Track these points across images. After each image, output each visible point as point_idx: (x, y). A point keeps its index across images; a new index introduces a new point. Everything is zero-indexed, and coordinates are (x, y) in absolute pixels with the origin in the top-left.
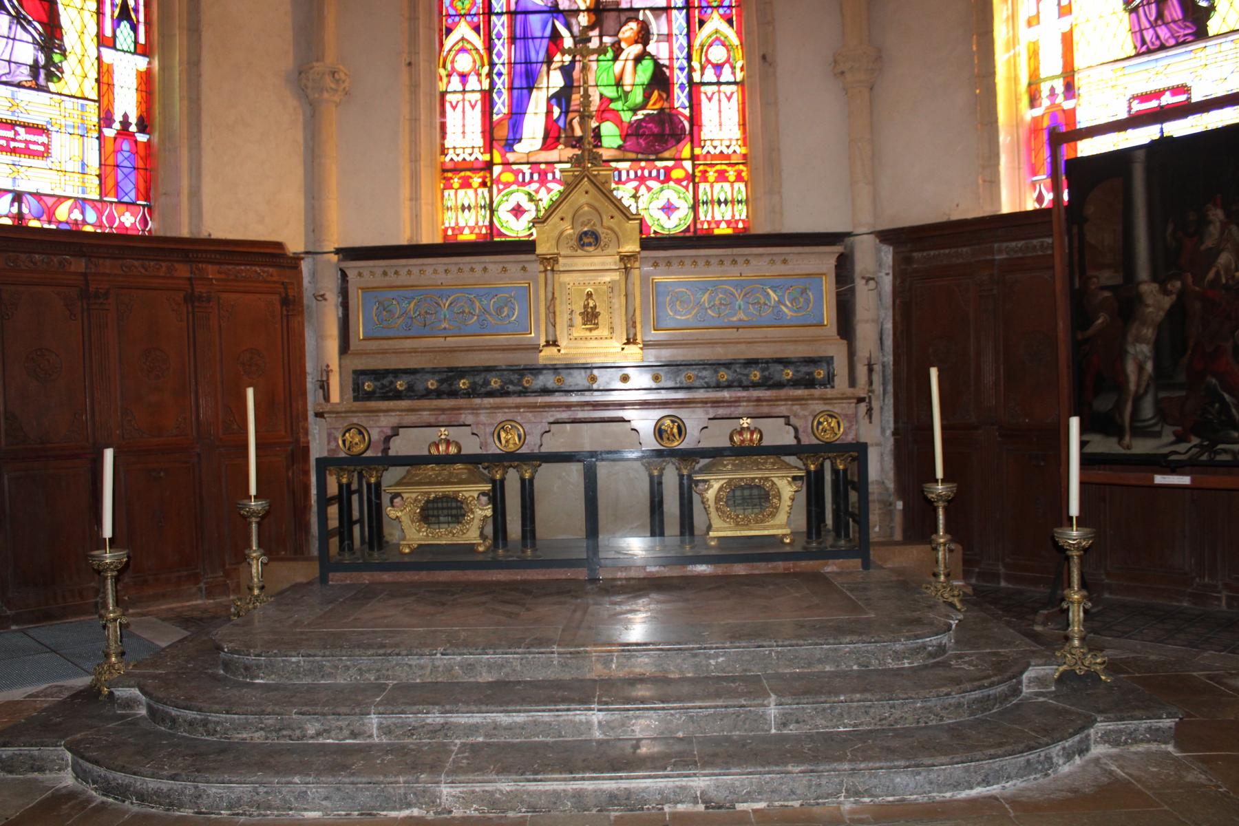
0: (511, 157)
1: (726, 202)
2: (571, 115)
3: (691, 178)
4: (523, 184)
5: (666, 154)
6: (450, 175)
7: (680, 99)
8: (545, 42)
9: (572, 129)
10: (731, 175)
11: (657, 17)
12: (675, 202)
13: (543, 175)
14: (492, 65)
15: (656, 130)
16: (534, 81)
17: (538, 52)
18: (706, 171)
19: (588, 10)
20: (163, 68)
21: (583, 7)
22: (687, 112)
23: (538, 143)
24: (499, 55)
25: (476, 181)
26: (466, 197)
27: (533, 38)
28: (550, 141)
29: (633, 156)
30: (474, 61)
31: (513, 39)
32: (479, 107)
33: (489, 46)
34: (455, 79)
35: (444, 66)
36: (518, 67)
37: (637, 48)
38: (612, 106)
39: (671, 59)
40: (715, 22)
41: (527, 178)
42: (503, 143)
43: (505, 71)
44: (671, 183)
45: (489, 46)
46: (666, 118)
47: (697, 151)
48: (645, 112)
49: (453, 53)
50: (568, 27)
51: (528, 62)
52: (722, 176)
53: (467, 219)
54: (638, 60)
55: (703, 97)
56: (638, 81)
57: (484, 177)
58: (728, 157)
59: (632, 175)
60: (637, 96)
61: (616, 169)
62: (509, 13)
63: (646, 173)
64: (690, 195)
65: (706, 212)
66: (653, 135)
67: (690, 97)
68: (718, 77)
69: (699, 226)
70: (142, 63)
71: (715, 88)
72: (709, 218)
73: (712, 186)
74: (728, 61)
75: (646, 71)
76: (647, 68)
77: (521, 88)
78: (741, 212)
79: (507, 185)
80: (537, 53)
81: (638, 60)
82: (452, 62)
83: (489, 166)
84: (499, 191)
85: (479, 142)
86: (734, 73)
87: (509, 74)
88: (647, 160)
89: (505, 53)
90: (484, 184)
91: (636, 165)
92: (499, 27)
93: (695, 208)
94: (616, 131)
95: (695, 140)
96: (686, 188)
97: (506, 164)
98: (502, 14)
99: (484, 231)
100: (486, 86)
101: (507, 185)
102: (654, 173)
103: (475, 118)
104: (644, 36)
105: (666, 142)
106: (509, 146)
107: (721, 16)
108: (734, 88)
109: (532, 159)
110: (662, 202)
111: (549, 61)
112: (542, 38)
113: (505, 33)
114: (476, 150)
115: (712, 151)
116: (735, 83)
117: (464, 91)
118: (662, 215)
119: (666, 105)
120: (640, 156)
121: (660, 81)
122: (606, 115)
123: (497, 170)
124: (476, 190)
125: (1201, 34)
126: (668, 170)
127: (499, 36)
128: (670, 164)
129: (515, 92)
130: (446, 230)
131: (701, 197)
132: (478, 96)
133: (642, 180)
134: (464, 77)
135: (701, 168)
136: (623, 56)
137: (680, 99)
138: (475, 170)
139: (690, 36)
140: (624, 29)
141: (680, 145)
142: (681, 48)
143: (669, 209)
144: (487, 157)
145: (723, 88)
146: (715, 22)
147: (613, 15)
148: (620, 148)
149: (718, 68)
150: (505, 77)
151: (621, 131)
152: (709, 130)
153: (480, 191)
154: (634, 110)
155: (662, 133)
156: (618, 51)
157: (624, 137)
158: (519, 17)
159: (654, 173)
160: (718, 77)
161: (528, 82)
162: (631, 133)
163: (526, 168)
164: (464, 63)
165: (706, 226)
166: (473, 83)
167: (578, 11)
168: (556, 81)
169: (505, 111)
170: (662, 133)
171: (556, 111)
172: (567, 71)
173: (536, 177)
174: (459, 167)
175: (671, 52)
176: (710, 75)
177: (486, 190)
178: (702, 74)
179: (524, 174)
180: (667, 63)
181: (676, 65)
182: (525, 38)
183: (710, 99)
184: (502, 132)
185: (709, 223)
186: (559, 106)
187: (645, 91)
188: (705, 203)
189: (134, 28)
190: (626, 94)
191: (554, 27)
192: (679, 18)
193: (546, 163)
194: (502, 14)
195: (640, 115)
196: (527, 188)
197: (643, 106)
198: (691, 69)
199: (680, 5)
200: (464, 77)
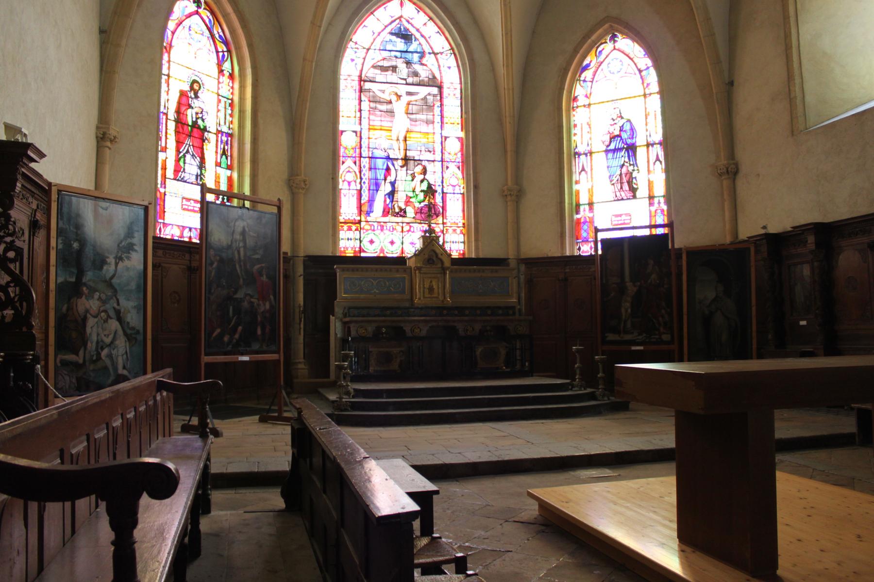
0: (369, 219)
7: (438, 199)
10: (458, 231)
13: (382, 227)
14: (361, 179)
17: (381, 175)
20: (239, 176)
22: (441, 204)
25: (354, 228)
26: (350, 234)
28: (386, 213)
31: (370, 169)
32: (355, 196)
33: (360, 172)
34: (346, 183)
37: (422, 177)
43: (367, 182)
50: (393, 165)
51: (376, 179)
53: (350, 244)
54: (422, 181)
70: (228, 173)
75: (424, 186)
76: (425, 183)
78: (461, 247)
79: (367, 230)
81: (422, 181)
83: (360, 222)
85: (356, 211)
90: (357, 230)
94: (413, 211)
97: (367, 222)
100: (359, 188)
101: (367, 230)
103: (354, 201)
104: (424, 171)
106: (368, 214)
111: (385, 180)
113: (367, 166)
121: (430, 191)
123: (363, 224)
125: (634, 197)
127: (364, 167)
132: (355, 192)
134: (349, 183)
144: (358, 218)
147: (412, 162)
150: (367, 184)
154: (420, 203)
156: (413, 177)
157: (416, 213)
162: (420, 211)
163: (376, 224)
164: (350, 177)
166: (353, 184)
167: (397, 159)
168: (389, 188)
169: (367, 199)
171: (388, 201)
172: (393, 184)
182: (375, 169)
184: (365, 208)
189: (227, 158)
195: (422, 204)
197: (424, 201)
200: (349, 183)
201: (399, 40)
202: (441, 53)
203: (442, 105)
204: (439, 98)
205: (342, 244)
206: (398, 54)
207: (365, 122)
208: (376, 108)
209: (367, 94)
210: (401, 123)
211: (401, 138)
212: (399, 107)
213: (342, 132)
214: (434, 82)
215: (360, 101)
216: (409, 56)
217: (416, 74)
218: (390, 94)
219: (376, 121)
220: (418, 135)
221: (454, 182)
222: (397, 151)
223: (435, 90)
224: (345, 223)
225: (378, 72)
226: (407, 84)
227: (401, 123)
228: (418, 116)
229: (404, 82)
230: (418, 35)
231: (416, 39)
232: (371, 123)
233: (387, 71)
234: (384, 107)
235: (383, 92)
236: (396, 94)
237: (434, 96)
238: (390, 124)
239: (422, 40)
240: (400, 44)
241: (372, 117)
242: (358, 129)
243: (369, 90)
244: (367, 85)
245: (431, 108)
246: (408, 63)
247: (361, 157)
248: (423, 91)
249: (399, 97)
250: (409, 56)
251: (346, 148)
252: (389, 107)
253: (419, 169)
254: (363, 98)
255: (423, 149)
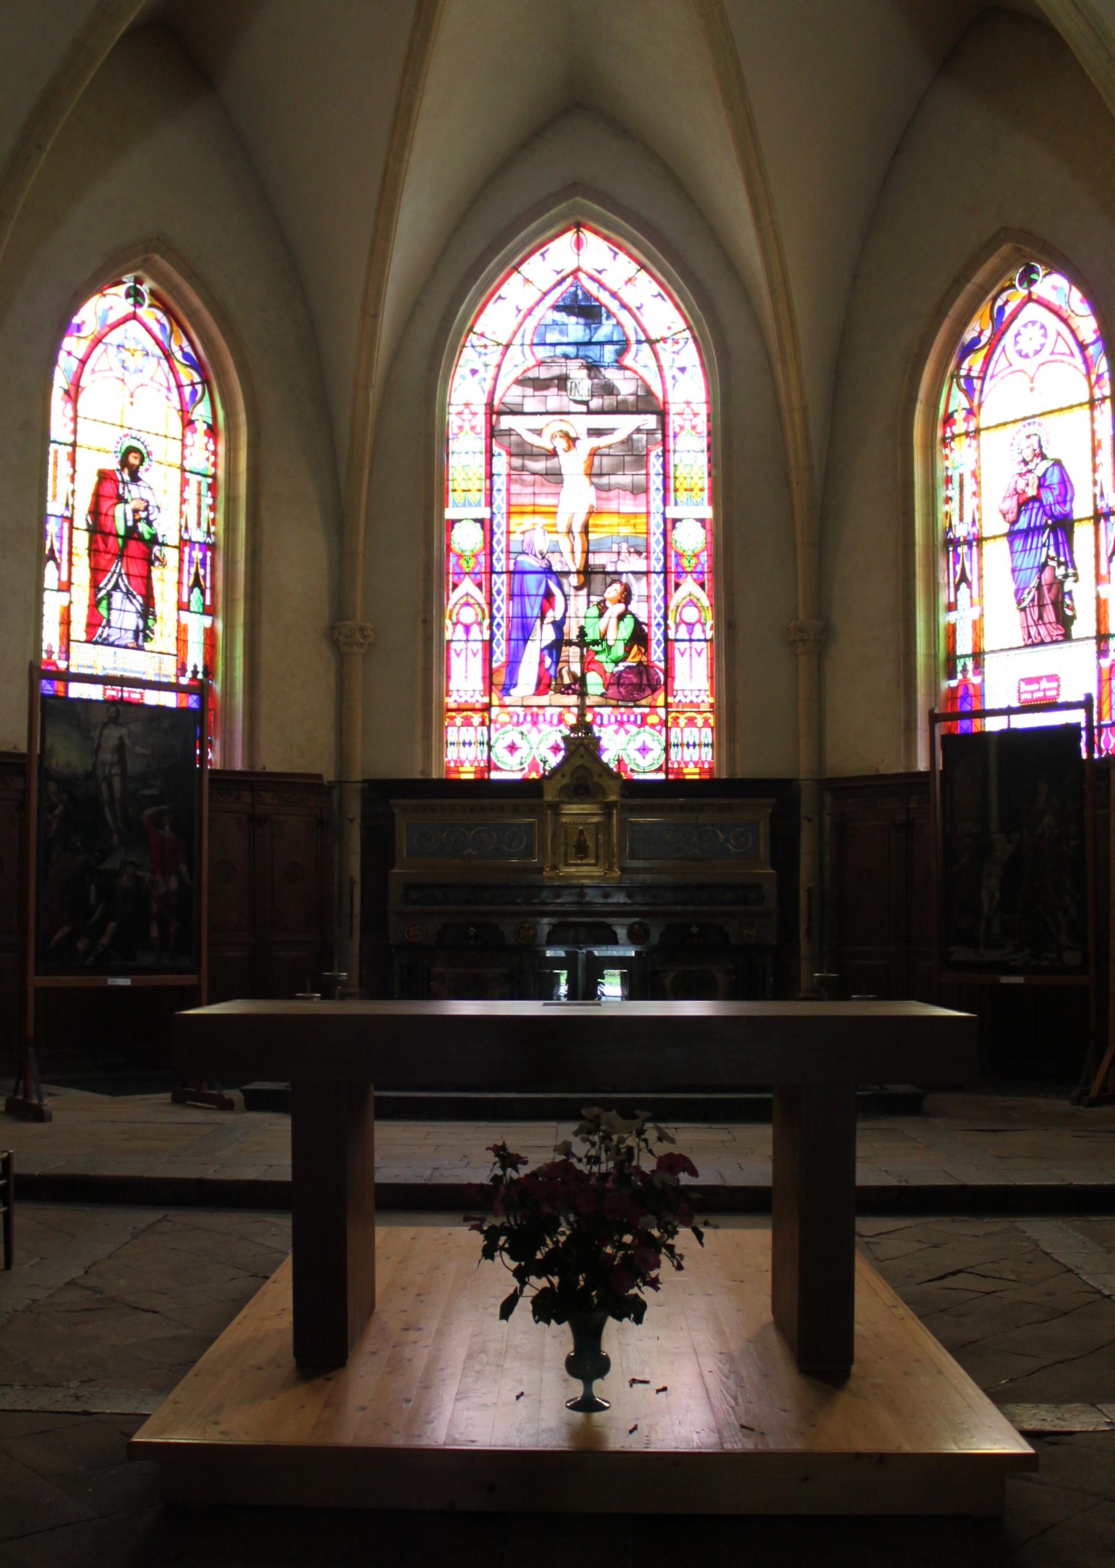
0: (507, 700)
1: (694, 745)
2: (561, 665)
3: (664, 723)
4: (518, 724)
5: (643, 702)
6: (453, 714)
7: (657, 654)
8: (539, 599)
9: (561, 677)
11: (638, 580)
12: (650, 744)
14: (492, 618)
15: (635, 680)
16: (529, 635)
17: (533, 608)
18: (678, 718)
19: (578, 572)
21: (574, 569)
22: (662, 665)
23: (532, 688)
24: (499, 609)
26: (468, 734)
27: (529, 596)
29: (613, 702)
30: (477, 614)
31: (511, 596)
33: (490, 603)
35: (450, 618)
36: (515, 620)
37: (621, 607)
38: (597, 658)
39: (649, 617)
40: (689, 586)
41: (521, 720)
42: (500, 687)
43: (504, 624)
44: (647, 728)
45: (490, 603)
46: (643, 669)
47: (670, 700)
48: (626, 664)
49: (458, 606)
50: (560, 586)
51: (524, 616)
52: (691, 722)
54: (621, 617)
55: (677, 652)
56: (620, 636)
57: (483, 718)
58: (698, 706)
59: (613, 719)
60: (619, 651)
61: (599, 714)
62: (508, 572)
63: (625, 718)
64: (663, 739)
65: (677, 753)
66: (632, 684)
67: (666, 652)
68: (690, 634)
69: (670, 765)
71: (687, 644)
72: (679, 759)
73: (682, 731)
74: (699, 621)
76: (629, 622)
77: (518, 640)
78: (707, 754)
79: (503, 725)
80: (532, 608)
81: (621, 617)
82: (458, 614)
83: (487, 708)
84: (496, 730)
85: (480, 686)
86: (704, 631)
87: (507, 627)
88: (625, 707)
89: (504, 607)
90: (483, 724)
91: (616, 711)
92: (499, 585)
93: (667, 749)
95: (668, 690)
96: (660, 732)
98: (502, 573)
99: (482, 764)
101: (503, 725)
102: (632, 718)
103: (476, 665)
104: (626, 596)
105: (643, 691)
106: (506, 690)
107: (695, 580)
108: (704, 644)
109: (526, 703)
110: (639, 744)
111: (543, 617)
112: (537, 595)
113: (504, 591)
114: (477, 693)
115: (684, 700)
116: (706, 640)
117: (467, 641)
118: (638, 756)
119: (644, 659)
120: (620, 703)
121: (639, 637)
122: (591, 666)
124: (476, 728)
126: (644, 717)
128: (647, 710)
129: (512, 643)
130: (449, 762)
131: (673, 740)
132: (479, 645)
133: (621, 723)
134: (467, 628)
135: (673, 714)
136: (607, 615)
137: (657, 654)
138: (474, 710)
139: (666, 599)
140: (609, 589)
141: (655, 695)
142: (658, 608)
143: (644, 750)
144: (486, 700)
145: (694, 644)
146: (689, 586)
147: (600, 577)
148: (602, 695)
149: (690, 626)
150: (503, 629)
151: (605, 680)
152: (680, 682)
153: (480, 729)
155: (640, 684)
156: (602, 609)
157: (607, 686)
158: (517, 576)
159: (632, 718)
160: (690, 634)
161: (523, 634)
162: (614, 682)
163: (520, 711)
165: (676, 766)
166: (475, 632)
169: (503, 659)
170: (640, 684)
171: (548, 661)
173: (529, 718)
174: (462, 707)
175: (649, 612)
176: (683, 633)
177: (485, 729)
178: (677, 632)
179: (518, 716)
180: (646, 621)
181: (654, 623)
182: (522, 595)
183: (682, 654)
184: (500, 678)
185: (679, 763)
186: (551, 656)
187: (626, 645)
188: (676, 745)
190: (610, 647)
191: (547, 586)
192: (657, 581)
193: (539, 707)
194: (502, 573)
196: (520, 728)
197: (624, 659)
198: (667, 627)
199: (658, 569)
201: (573, 319)
202: (664, 340)
203: (665, 452)
204: (659, 436)
205: (452, 754)
206: (571, 350)
207: (500, 499)
208: (523, 468)
209: (505, 440)
210: (576, 496)
211: (577, 528)
212: (572, 463)
213: (452, 523)
214: (648, 403)
215: (490, 455)
216: (594, 352)
217: (609, 389)
218: (553, 437)
219: (523, 496)
220: (614, 520)
221: (690, 615)
222: (567, 557)
223: (650, 421)
224: (459, 710)
225: (529, 391)
226: (590, 412)
227: (576, 496)
228: (614, 479)
229: (584, 408)
230: (613, 305)
231: (610, 315)
232: (513, 501)
233: (547, 388)
234: (539, 465)
235: (539, 432)
236: (566, 436)
237: (650, 432)
238: (551, 501)
239: (623, 316)
240: (576, 329)
241: (515, 488)
242: (485, 513)
243: (509, 432)
244: (506, 422)
245: (641, 460)
246: (593, 368)
247: (491, 571)
248: (625, 425)
249: (572, 441)
250: (594, 352)
251: (459, 556)
252: (552, 463)
253: (614, 591)
254: (496, 449)
255: (624, 546)
